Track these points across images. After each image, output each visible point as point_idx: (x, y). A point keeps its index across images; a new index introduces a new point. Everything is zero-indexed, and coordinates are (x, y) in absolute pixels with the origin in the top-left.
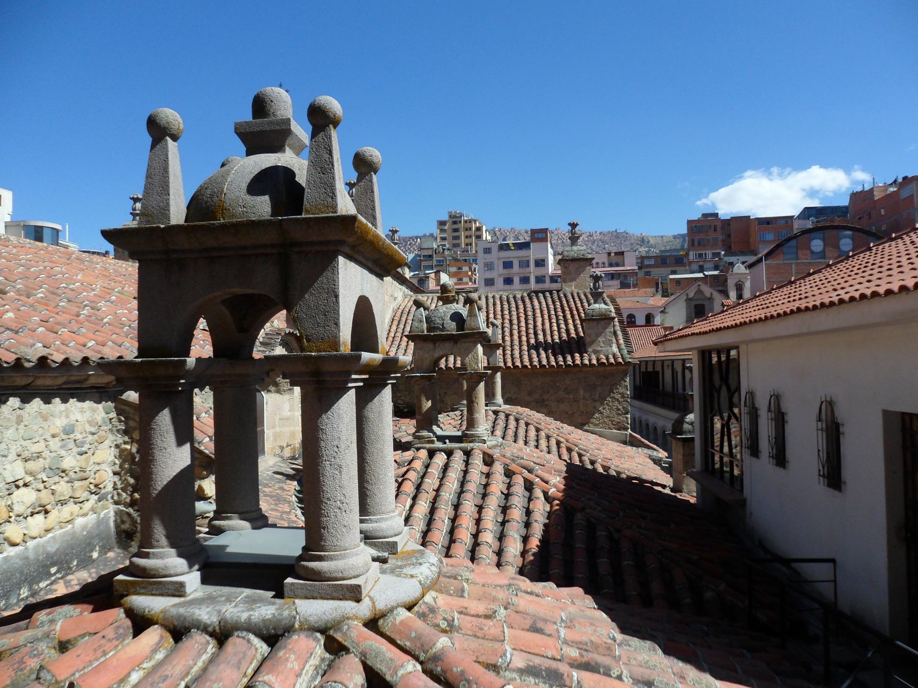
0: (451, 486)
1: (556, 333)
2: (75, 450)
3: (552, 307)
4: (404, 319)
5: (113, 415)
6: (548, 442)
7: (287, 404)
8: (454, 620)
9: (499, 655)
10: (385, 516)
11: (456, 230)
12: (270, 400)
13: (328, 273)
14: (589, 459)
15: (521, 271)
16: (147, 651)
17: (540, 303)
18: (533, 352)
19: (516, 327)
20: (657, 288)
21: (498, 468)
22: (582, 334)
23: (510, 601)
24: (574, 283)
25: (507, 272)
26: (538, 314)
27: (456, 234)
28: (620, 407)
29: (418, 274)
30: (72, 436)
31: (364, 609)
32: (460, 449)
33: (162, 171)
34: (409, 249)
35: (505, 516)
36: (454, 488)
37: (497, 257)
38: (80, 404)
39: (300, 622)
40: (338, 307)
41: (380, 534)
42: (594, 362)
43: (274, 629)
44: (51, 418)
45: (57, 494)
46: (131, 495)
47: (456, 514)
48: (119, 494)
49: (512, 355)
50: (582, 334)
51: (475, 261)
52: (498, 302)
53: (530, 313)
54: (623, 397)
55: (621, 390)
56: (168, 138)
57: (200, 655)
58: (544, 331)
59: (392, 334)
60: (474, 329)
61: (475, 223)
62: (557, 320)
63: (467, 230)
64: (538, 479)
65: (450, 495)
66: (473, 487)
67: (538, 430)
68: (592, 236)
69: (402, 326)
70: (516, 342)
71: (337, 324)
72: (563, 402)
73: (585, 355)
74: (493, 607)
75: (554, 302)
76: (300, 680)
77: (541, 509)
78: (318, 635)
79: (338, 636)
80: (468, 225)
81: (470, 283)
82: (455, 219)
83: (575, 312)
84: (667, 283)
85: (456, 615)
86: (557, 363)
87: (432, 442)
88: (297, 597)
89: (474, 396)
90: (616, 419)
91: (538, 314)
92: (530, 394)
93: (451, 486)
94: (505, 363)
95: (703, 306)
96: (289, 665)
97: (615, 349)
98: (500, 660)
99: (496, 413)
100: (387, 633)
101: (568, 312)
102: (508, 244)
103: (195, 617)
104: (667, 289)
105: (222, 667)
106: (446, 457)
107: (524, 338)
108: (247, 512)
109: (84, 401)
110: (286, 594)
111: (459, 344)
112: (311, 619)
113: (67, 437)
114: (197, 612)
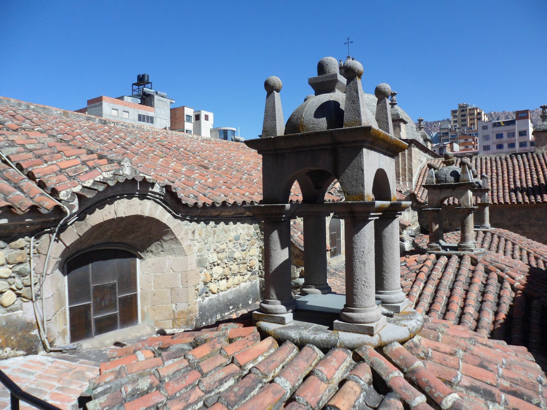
1: (530, 181)
2: (240, 248)
3: (527, 163)
5: (258, 231)
6: (521, 252)
8: (428, 353)
9: (453, 376)
13: (358, 158)
15: (509, 139)
16: (266, 348)
17: (518, 161)
19: (500, 177)
21: (481, 268)
23: (468, 347)
24: (544, 147)
25: (498, 141)
29: (439, 145)
30: (238, 241)
31: (375, 340)
32: (456, 254)
34: (434, 129)
35: (483, 298)
37: (492, 132)
38: (242, 225)
39: (340, 343)
40: (364, 176)
41: (391, 301)
43: (326, 345)
44: (229, 232)
45: (232, 270)
48: (261, 272)
49: (498, 196)
52: (489, 162)
53: (511, 168)
56: (274, 91)
57: (290, 353)
60: (466, 181)
61: (477, 110)
62: (531, 172)
63: (471, 115)
64: (507, 276)
65: (448, 282)
67: (514, 244)
71: (363, 186)
75: (528, 160)
76: (337, 372)
77: (508, 296)
78: (349, 351)
79: (360, 353)
80: (472, 112)
82: (463, 108)
85: (430, 351)
86: (530, 200)
87: (439, 250)
88: (339, 330)
94: (493, 200)
96: (332, 364)
98: (454, 379)
99: (485, 232)
100: (388, 355)
102: (500, 122)
103: (289, 335)
105: (300, 360)
106: (447, 259)
107: (506, 185)
108: (320, 285)
109: (244, 223)
110: (334, 328)
111: (456, 190)
112: (346, 342)
113: (236, 242)
114: (290, 332)
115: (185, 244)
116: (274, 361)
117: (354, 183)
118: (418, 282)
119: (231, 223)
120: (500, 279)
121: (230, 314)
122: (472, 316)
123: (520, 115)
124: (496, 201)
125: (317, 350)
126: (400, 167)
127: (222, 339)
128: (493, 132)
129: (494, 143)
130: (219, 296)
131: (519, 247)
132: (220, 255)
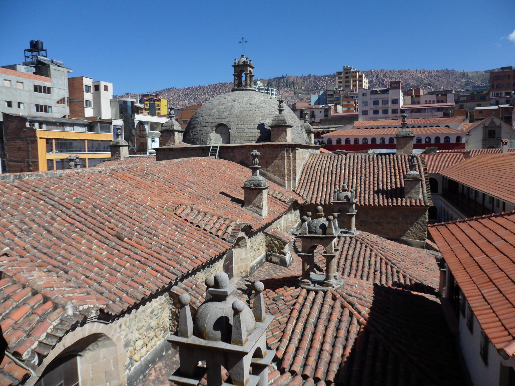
1: (389, 184)
2: (155, 317)
3: (388, 166)
4: (308, 172)
6: (376, 258)
7: (244, 252)
11: (347, 77)
13: (240, 362)
18: (376, 195)
19: (367, 179)
20: (467, 116)
22: (403, 185)
24: (402, 150)
26: (381, 172)
27: (347, 80)
28: (422, 228)
30: (154, 313)
34: (321, 83)
37: (369, 98)
42: (408, 204)
47: (315, 330)
49: (364, 197)
50: (403, 185)
51: (357, 97)
53: (376, 171)
54: (423, 223)
55: (423, 219)
58: (383, 182)
59: (302, 181)
61: (359, 73)
62: (391, 175)
63: (353, 77)
65: (313, 319)
66: (324, 316)
67: (371, 251)
68: (431, 73)
69: (307, 176)
70: (367, 189)
73: (404, 199)
77: (355, 329)
80: (354, 74)
81: (355, 111)
82: (347, 71)
83: (401, 171)
84: (473, 112)
86: (388, 203)
87: (309, 285)
90: (419, 234)
91: (381, 172)
92: (373, 219)
95: (494, 131)
97: (421, 196)
99: (351, 238)
101: (397, 171)
104: (473, 116)
107: (372, 187)
109: (157, 298)
115: (114, 339)
118: (291, 319)
120: (351, 314)
122: (328, 351)
123: (393, 85)
124: (362, 203)
126: (286, 169)
128: (371, 99)
129: (371, 109)
132: (141, 331)
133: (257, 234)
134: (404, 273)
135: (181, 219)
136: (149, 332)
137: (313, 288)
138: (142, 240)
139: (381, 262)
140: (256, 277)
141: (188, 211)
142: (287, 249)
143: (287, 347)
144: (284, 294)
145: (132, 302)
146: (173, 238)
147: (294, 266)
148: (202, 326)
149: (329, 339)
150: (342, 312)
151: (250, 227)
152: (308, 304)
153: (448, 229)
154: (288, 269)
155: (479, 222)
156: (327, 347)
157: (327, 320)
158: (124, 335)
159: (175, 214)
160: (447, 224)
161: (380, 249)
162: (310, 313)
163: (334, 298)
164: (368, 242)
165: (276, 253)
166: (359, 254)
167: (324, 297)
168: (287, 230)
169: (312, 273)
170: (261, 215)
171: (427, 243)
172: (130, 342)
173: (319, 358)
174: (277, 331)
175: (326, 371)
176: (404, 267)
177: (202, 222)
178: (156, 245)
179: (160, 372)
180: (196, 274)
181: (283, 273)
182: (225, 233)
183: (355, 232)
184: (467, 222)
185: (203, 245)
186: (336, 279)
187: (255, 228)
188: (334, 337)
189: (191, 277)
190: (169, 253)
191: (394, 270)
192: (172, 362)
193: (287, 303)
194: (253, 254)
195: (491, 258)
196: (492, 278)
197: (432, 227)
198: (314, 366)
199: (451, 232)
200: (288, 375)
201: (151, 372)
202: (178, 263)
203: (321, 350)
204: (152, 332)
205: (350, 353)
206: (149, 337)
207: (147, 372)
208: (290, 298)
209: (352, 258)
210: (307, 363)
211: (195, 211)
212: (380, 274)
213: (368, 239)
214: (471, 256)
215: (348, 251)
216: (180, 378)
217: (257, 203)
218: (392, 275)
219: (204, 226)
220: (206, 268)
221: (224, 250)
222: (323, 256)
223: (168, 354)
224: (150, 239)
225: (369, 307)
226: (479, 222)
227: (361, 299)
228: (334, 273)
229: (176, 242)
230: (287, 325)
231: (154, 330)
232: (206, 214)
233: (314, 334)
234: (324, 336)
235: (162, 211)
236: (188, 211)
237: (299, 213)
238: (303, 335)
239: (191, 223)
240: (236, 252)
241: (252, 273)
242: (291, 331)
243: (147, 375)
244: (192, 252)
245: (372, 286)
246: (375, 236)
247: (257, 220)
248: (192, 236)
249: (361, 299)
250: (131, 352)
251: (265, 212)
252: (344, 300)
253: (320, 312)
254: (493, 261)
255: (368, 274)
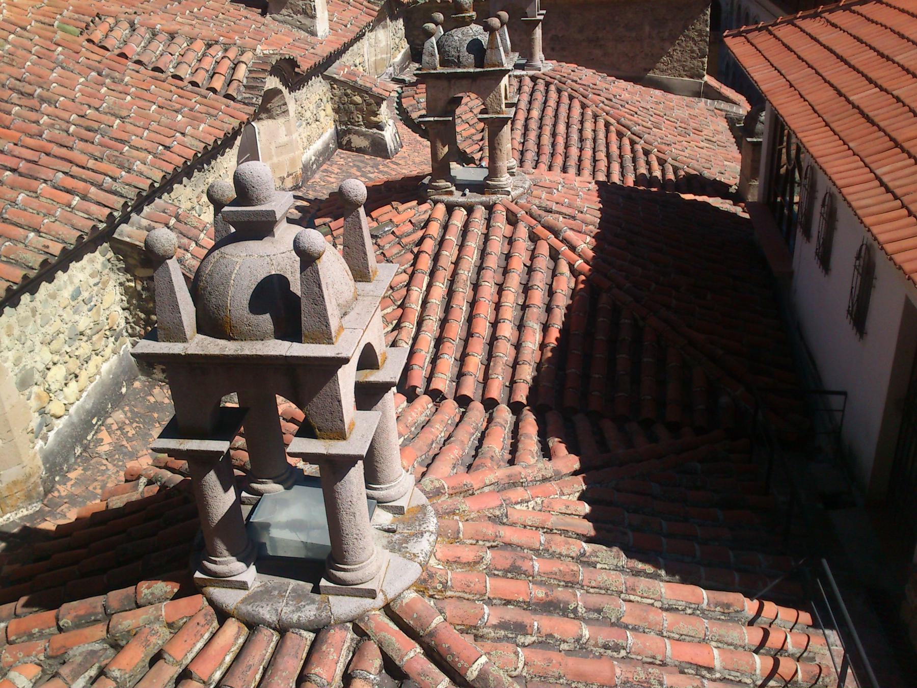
0: (470, 260)
2: (86, 308)
6: (595, 123)
7: (283, 128)
10: (393, 484)
12: (262, 128)
14: (643, 148)
28: (695, 48)
30: (80, 298)
31: (380, 601)
33: (169, 291)
35: (526, 298)
36: (473, 262)
46: (145, 329)
47: (475, 295)
48: (131, 327)
54: (700, 35)
65: (469, 271)
66: (493, 262)
67: (584, 106)
72: (623, 41)
74: (481, 554)
76: (339, 664)
77: (565, 284)
79: (362, 625)
87: (451, 193)
89: (496, 142)
93: (470, 260)
96: (331, 657)
99: (534, 79)
103: (261, 616)
105: (286, 658)
106: (465, 213)
108: (278, 476)
112: (342, 617)
113: (76, 301)
114: (261, 610)
116: (251, 665)
117: (329, 417)
118: (418, 276)
119: (60, 272)
120: (553, 252)
121: (96, 432)
122: (509, 340)
125: (305, 634)
127: (156, 626)
130: (70, 416)
131: (593, 112)
132: (55, 345)
133: (310, 82)
134: (660, 155)
135: (108, 54)
136: (77, 343)
137: (462, 200)
138: (9, 113)
139: (607, 131)
140: (318, 188)
141: (122, 31)
142: (386, 113)
143: (415, 339)
144: (394, 220)
145: (18, 274)
146: (96, 103)
147: (406, 155)
148: (218, 307)
149: (509, 312)
150: (533, 250)
151: (292, 63)
152: (453, 237)
153: (775, 37)
154: (392, 162)
155: (854, 12)
156: (507, 330)
157: (501, 270)
158: (11, 359)
159: (89, 41)
160: (772, 26)
161: (603, 102)
162: (459, 258)
163: (512, 220)
164: (576, 86)
165: (359, 126)
166: (556, 116)
167: (488, 220)
168: (379, 71)
169: (454, 165)
170: (313, 34)
171: (706, 82)
172: (33, 375)
173: (490, 355)
174: (388, 307)
175: (507, 384)
176: (659, 140)
177: (167, 58)
178: (52, 126)
179: (122, 433)
180: (172, 190)
181: (381, 172)
182: (231, 81)
183: (544, 65)
184: (823, 15)
185: (180, 117)
186: (512, 174)
187: (305, 65)
188: (519, 307)
189: (160, 198)
190: (93, 143)
191: (638, 147)
192: (148, 407)
193: (405, 241)
194: (304, 132)
195: (894, 93)
196: (899, 138)
197: (734, 36)
198: (480, 376)
199: (784, 44)
200: (424, 403)
201: (100, 436)
202: (122, 167)
203: (493, 339)
204: (83, 344)
205: (557, 339)
206: (77, 357)
207: (89, 438)
208: (409, 228)
209: (540, 128)
210: (465, 370)
211: (142, 30)
212: (605, 159)
213: (575, 78)
214: (840, 94)
215: (529, 111)
216: (181, 441)
217: (301, 3)
218: (634, 160)
219: (174, 68)
220: (196, 173)
221: (235, 123)
222: (480, 120)
223: (135, 389)
224: (32, 109)
225: (592, 235)
226: (854, 12)
227: (574, 218)
228: (508, 160)
229: (106, 113)
230: (408, 291)
231: (90, 338)
232: (172, 36)
233: (473, 304)
234: (498, 306)
235: (50, 34)
236: (122, 31)
237: (403, 28)
238: (448, 308)
239: (138, 62)
240: (262, 128)
241: (308, 180)
242: (420, 302)
243: (92, 444)
244: (154, 135)
245: (593, 187)
246: (590, 72)
247: (307, 47)
248: (146, 95)
249: (574, 218)
250: (39, 397)
251: (322, 26)
252: (534, 222)
253: (483, 254)
254: (898, 100)
255: (580, 160)
